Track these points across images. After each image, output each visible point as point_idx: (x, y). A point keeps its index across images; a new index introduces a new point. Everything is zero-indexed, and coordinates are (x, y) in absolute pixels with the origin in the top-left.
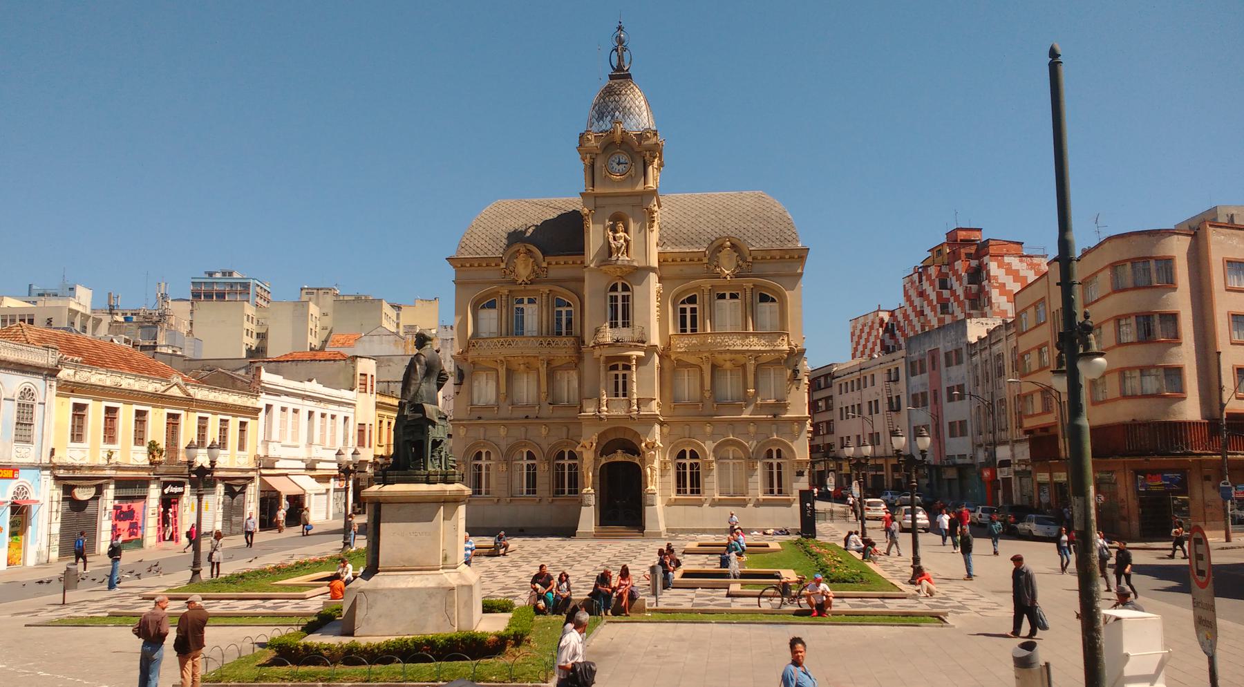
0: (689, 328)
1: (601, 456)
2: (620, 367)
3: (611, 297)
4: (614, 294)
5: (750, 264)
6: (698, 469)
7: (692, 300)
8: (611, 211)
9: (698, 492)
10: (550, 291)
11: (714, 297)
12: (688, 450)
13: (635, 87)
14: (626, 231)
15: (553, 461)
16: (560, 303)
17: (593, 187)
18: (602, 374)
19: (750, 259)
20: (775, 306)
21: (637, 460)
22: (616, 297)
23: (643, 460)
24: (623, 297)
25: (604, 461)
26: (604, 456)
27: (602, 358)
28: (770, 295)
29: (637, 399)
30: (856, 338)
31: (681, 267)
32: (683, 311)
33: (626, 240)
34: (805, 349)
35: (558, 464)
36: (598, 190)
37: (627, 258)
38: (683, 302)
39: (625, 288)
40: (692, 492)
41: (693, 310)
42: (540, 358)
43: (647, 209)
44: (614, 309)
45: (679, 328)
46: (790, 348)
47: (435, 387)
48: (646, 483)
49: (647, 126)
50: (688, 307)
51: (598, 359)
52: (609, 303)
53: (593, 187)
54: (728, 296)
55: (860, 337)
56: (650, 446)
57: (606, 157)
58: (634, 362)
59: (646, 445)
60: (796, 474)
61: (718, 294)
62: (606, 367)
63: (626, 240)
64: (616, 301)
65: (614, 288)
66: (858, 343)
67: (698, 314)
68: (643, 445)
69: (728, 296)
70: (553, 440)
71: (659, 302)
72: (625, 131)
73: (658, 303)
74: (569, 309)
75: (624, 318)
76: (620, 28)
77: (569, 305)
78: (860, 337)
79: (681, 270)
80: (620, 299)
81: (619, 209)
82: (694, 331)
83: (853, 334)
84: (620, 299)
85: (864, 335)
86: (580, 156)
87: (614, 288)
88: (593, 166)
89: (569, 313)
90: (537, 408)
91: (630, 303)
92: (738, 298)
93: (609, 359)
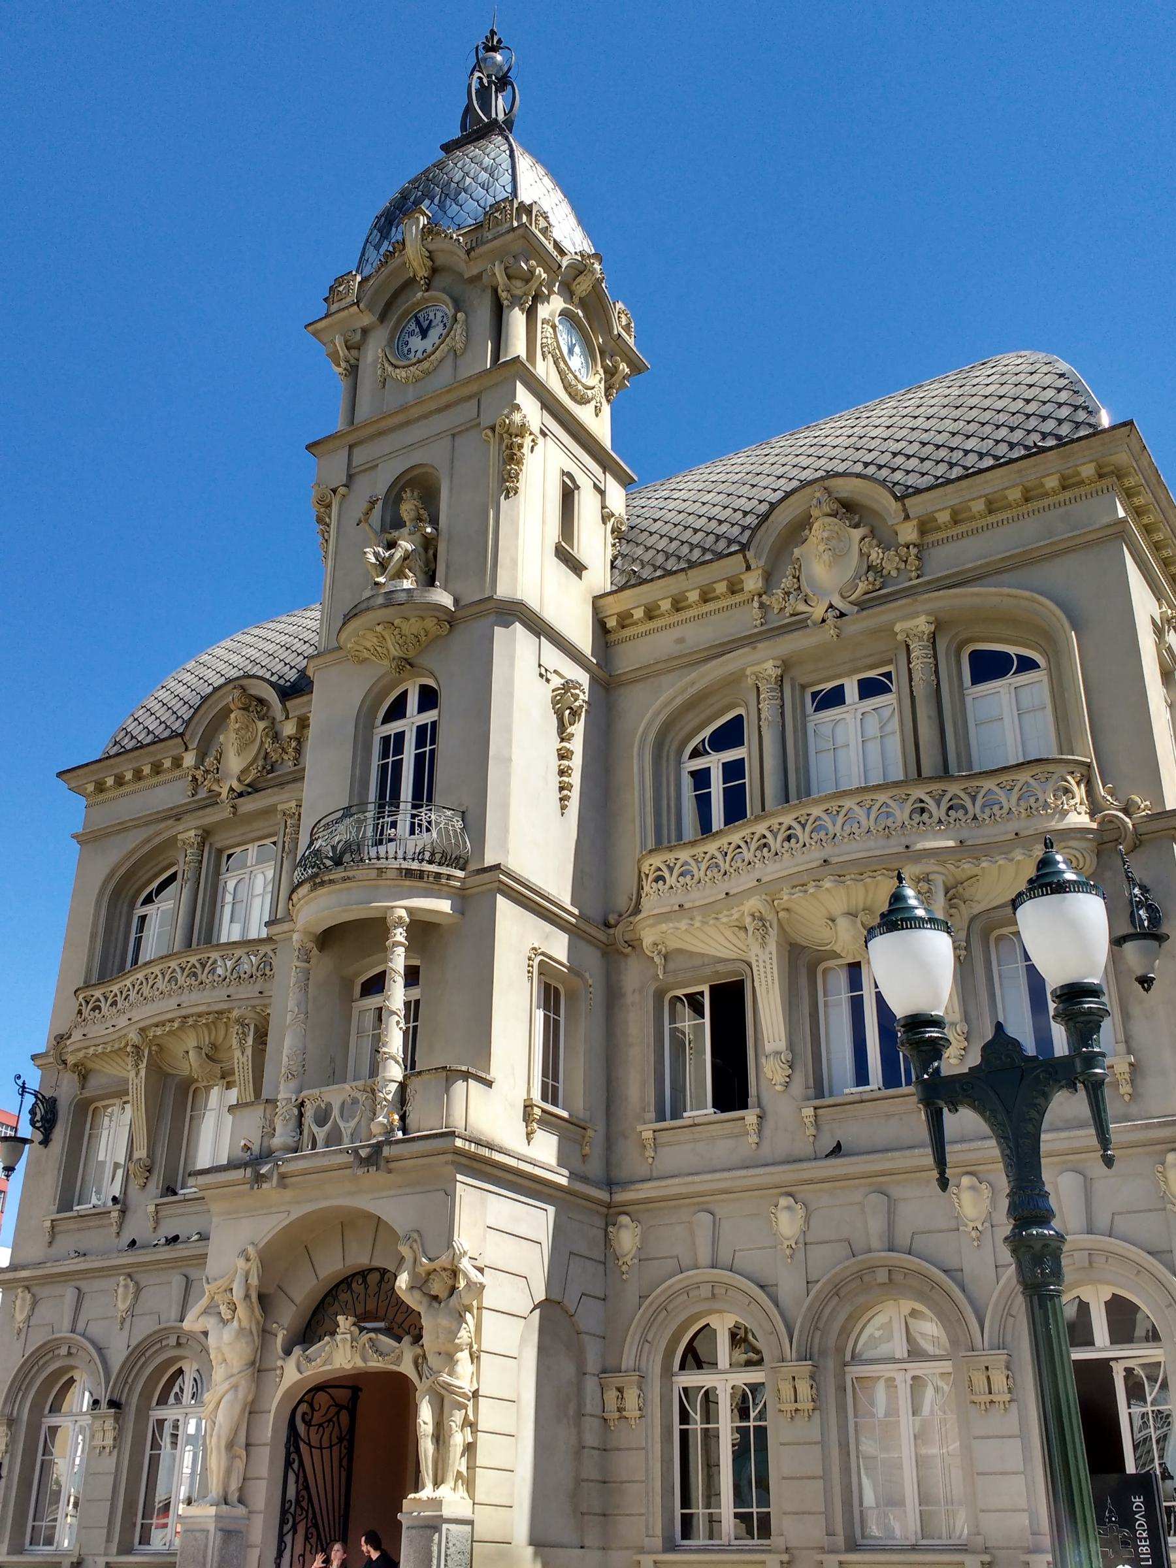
1: (288, 1352)
3: (386, 740)
12: (722, 1325)
20: (1035, 684)
26: (297, 1351)
28: (1012, 650)
31: (677, 632)
43: (493, 429)
50: (715, 762)
54: (851, 691)
58: (400, 935)
61: (814, 695)
64: (399, 750)
69: (851, 691)
79: (681, 640)
81: (416, 458)
92: (890, 690)
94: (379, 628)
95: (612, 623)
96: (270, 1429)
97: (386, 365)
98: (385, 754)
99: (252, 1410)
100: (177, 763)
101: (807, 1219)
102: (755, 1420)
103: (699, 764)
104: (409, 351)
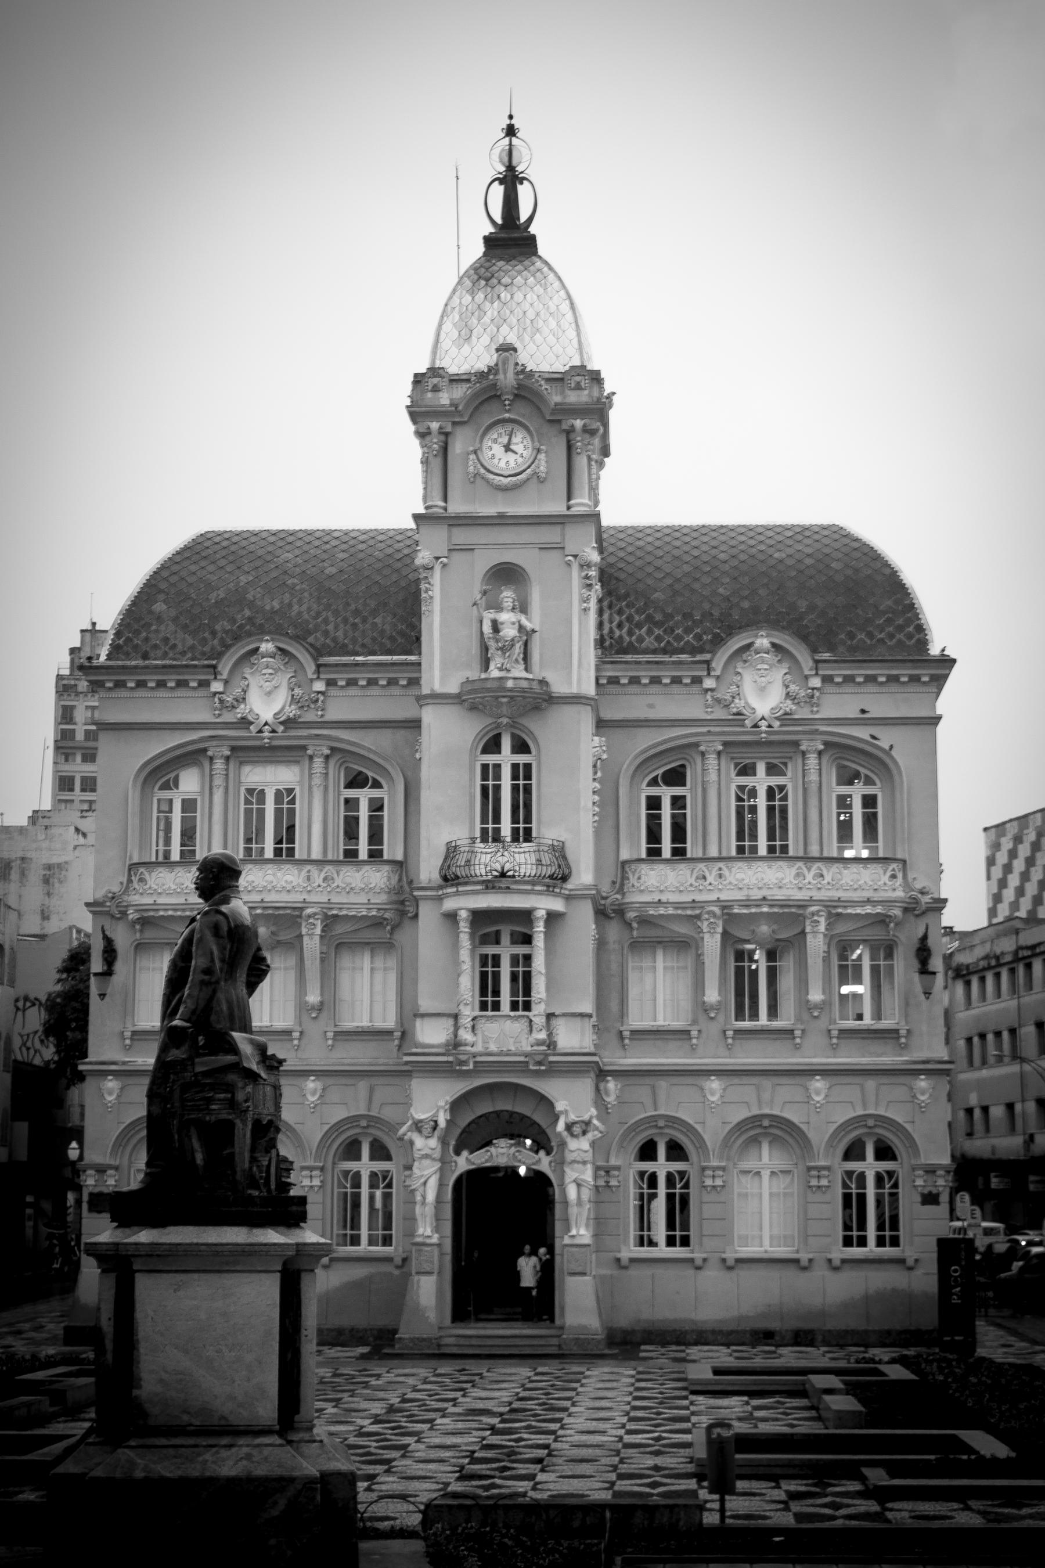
0: (666, 846)
1: (458, 1153)
2: (505, 939)
4: (491, 759)
5: (817, 694)
6: (686, 1186)
7: (675, 777)
8: (485, 561)
9: (685, 1242)
10: (333, 749)
11: (728, 774)
13: (546, 269)
14: (523, 608)
15: (334, 1163)
16: (357, 781)
17: (445, 500)
18: (465, 954)
19: (816, 682)
21: (544, 1163)
22: (498, 767)
23: (560, 1164)
24: (515, 767)
25: (464, 1163)
26: (465, 1153)
27: (463, 914)
29: (550, 1016)
30: (997, 872)
32: (654, 803)
33: (521, 628)
34: (945, 901)
35: (346, 1173)
36: (457, 506)
37: (525, 675)
38: (654, 782)
39: (521, 747)
40: (671, 1242)
41: (678, 802)
42: (309, 911)
44: (489, 796)
45: (644, 845)
46: (910, 897)
47: (245, 991)
48: (566, 1220)
49: (577, 362)
50: (666, 793)
51: (452, 917)
52: (478, 782)
53: (445, 500)
55: (1008, 869)
56: (577, 1129)
57: (477, 431)
59: (569, 1127)
60: (919, 1199)
62: (472, 935)
63: (521, 628)
64: (498, 776)
65: (493, 745)
66: (1003, 883)
67: (688, 811)
68: (561, 1126)
70: (340, 1114)
71: (600, 781)
72: (523, 371)
73: (597, 785)
74: (376, 793)
75: (515, 819)
76: (511, 131)
77: (377, 785)
78: (1008, 869)
79: (651, 706)
80: (506, 773)
82: (679, 853)
83: (991, 862)
84: (506, 773)
85: (1019, 865)
86: (411, 428)
87: (493, 745)
88: (445, 450)
89: (377, 806)
90: (296, 1035)
91: (534, 782)
93: (479, 917)
94: (505, 700)
95: (604, 681)
96: (449, 1195)
97: (479, 466)
98: (485, 777)
99: (441, 1185)
100: (204, 684)
101: (724, 1090)
102: (681, 1188)
103: (654, 791)
104: (493, 455)
